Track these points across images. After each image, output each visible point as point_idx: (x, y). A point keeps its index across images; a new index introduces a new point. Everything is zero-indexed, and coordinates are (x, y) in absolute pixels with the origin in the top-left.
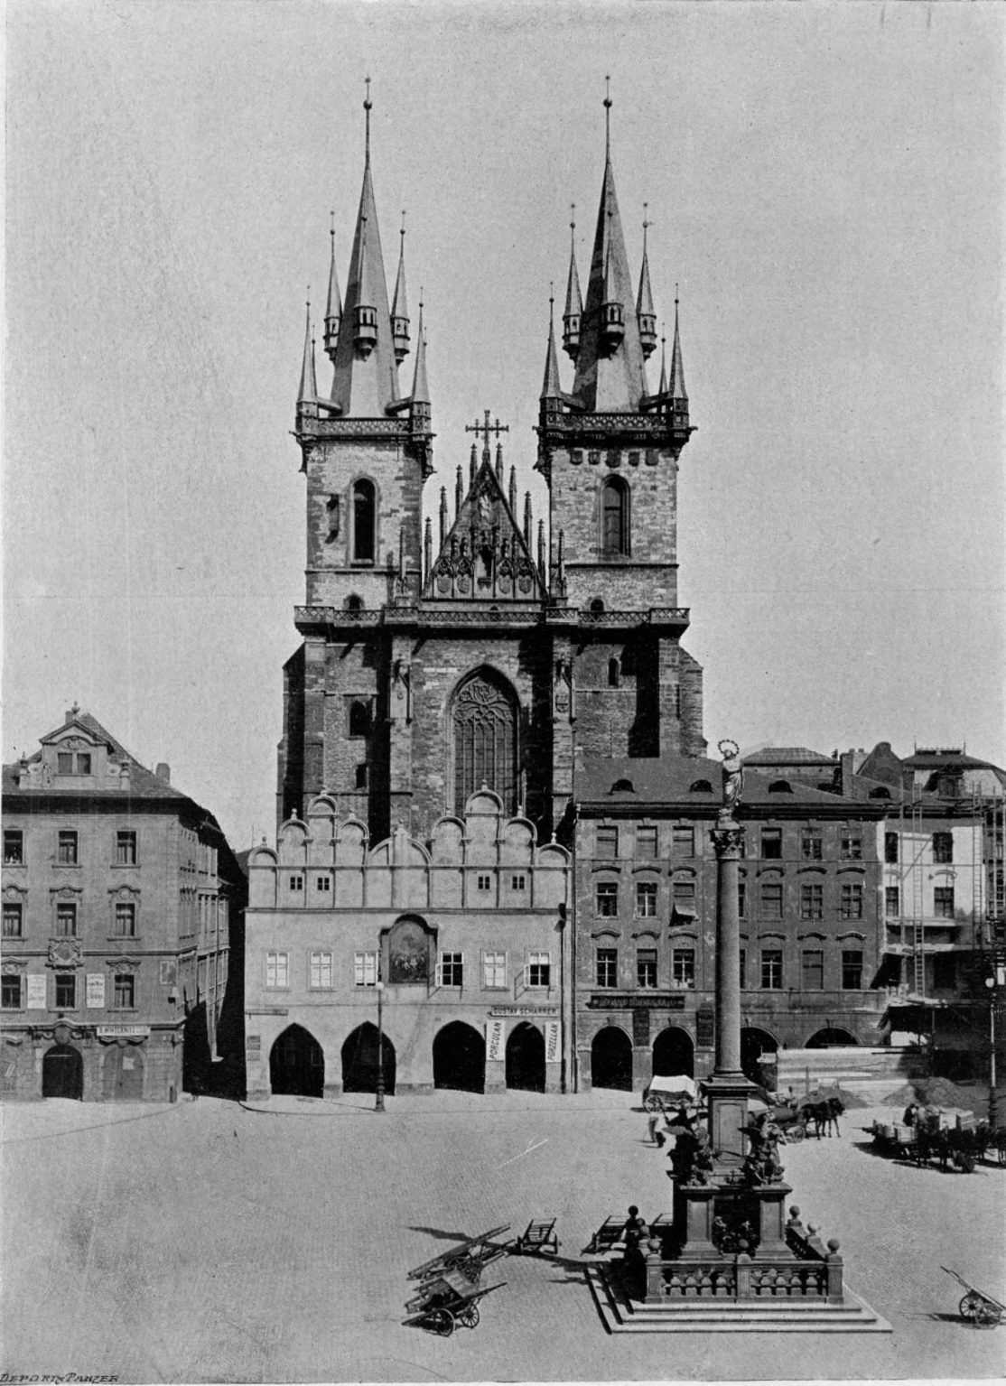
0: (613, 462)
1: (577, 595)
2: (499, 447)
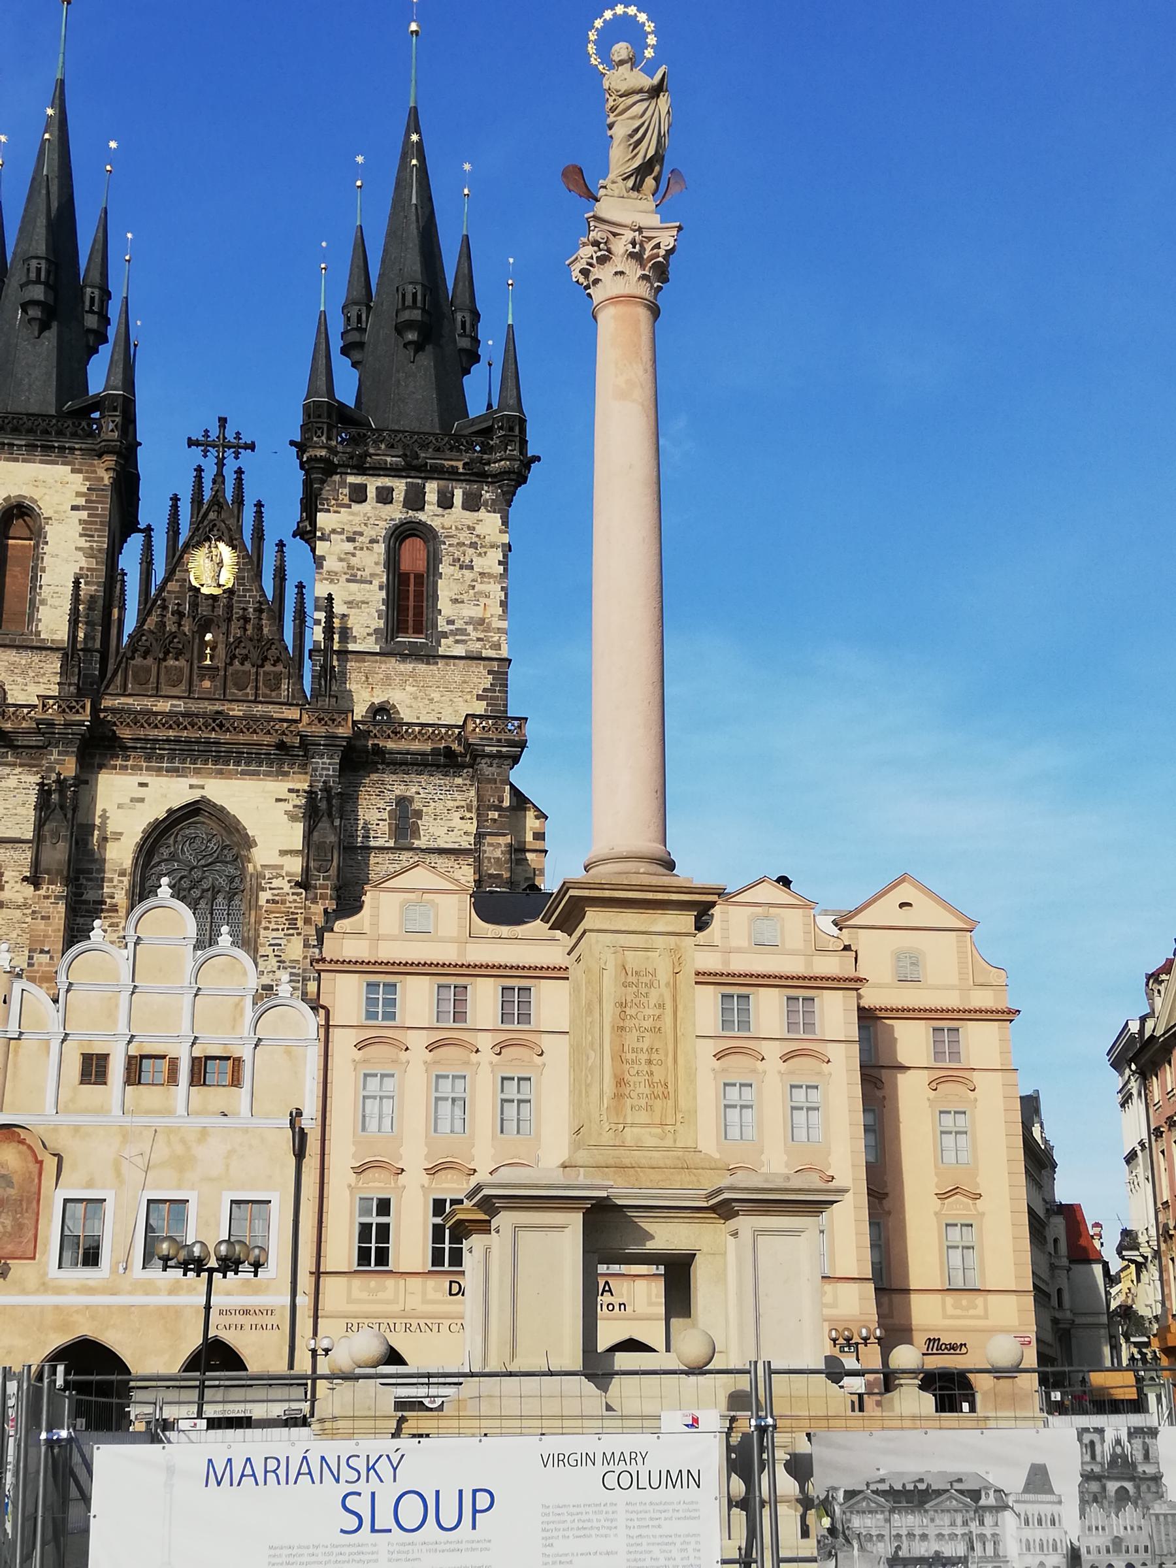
0: (415, 501)
2: (240, 472)
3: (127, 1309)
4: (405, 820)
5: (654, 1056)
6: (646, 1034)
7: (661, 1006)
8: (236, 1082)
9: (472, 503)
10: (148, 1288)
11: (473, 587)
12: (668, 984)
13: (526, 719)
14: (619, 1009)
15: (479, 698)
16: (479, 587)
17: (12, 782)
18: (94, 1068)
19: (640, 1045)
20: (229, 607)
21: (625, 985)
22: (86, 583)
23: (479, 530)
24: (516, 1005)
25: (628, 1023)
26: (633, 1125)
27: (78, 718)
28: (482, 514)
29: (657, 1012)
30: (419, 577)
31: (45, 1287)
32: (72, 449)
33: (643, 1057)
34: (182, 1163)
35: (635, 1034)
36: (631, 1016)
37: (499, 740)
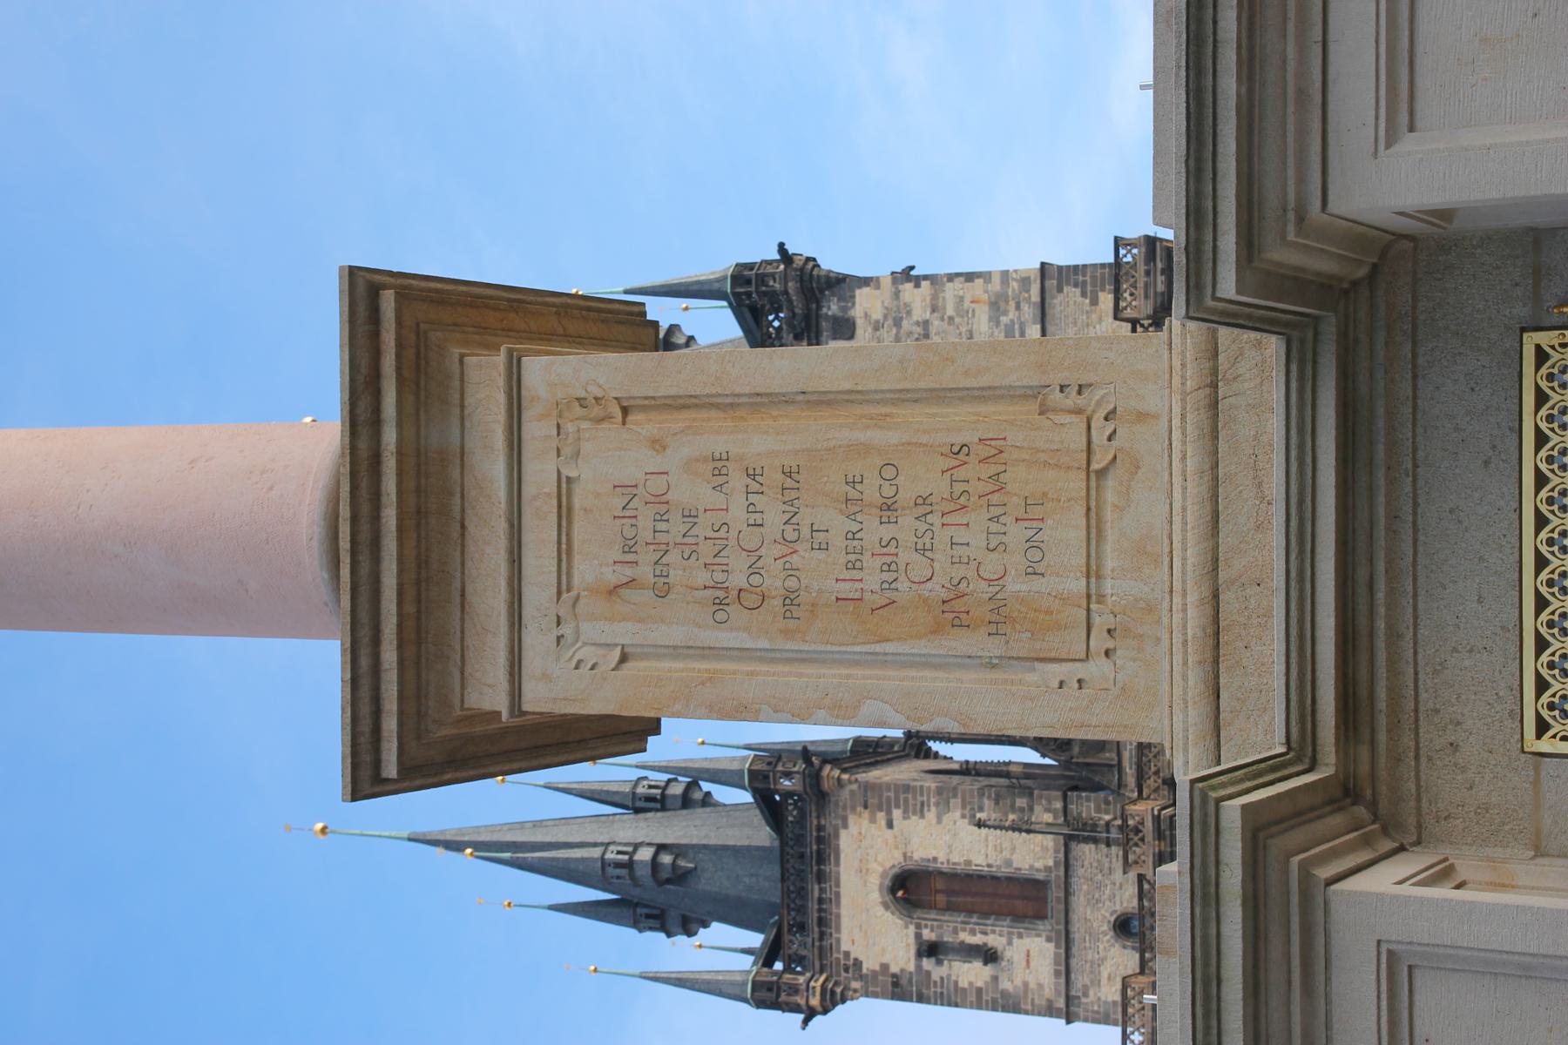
5: (871, 490)
6: (806, 517)
7: (719, 465)
9: (845, 328)
11: (951, 318)
12: (658, 445)
13: (1116, 239)
14: (734, 609)
15: (1095, 302)
16: (950, 311)
19: (837, 539)
21: (663, 592)
22: (981, 809)
23: (877, 315)
25: (774, 581)
26: (1092, 572)
27: (1149, 824)
28: (857, 312)
29: (737, 481)
32: (820, 828)
33: (874, 531)
35: (804, 557)
36: (753, 571)
37: (1148, 273)
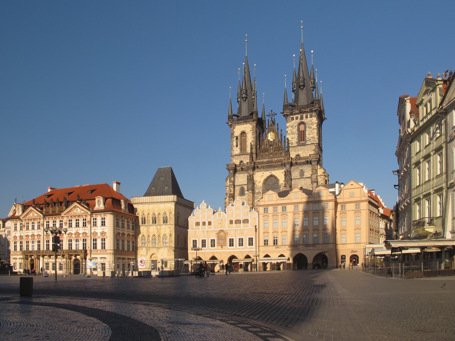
1: (293, 155)
3: (237, 251)
4: (302, 173)
8: (248, 223)
10: (239, 249)
17: (245, 176)
18: (231, 222)
20: (274, 142)
24: (284, 209)
30: (303, 131)
31: (228, 249)
34: (242, 233)
